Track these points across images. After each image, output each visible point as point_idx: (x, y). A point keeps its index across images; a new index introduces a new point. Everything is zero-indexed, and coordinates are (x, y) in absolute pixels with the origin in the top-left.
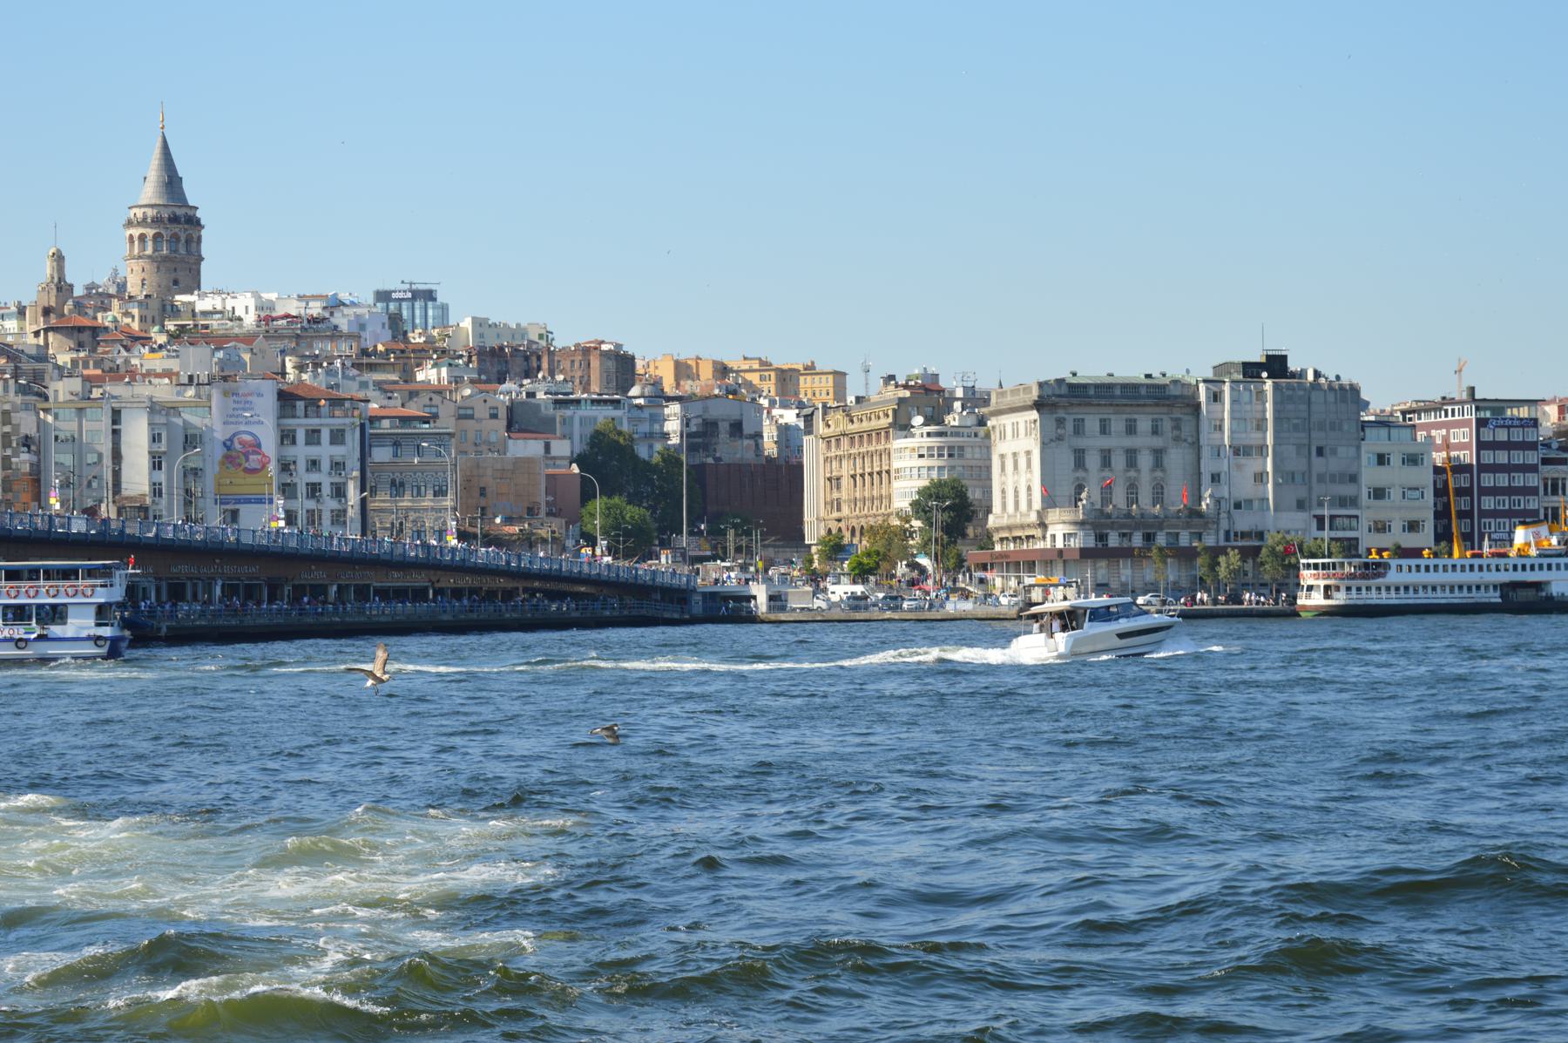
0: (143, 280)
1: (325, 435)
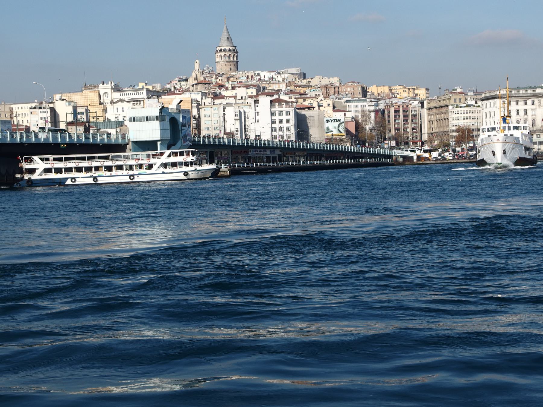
1: (284, 113)
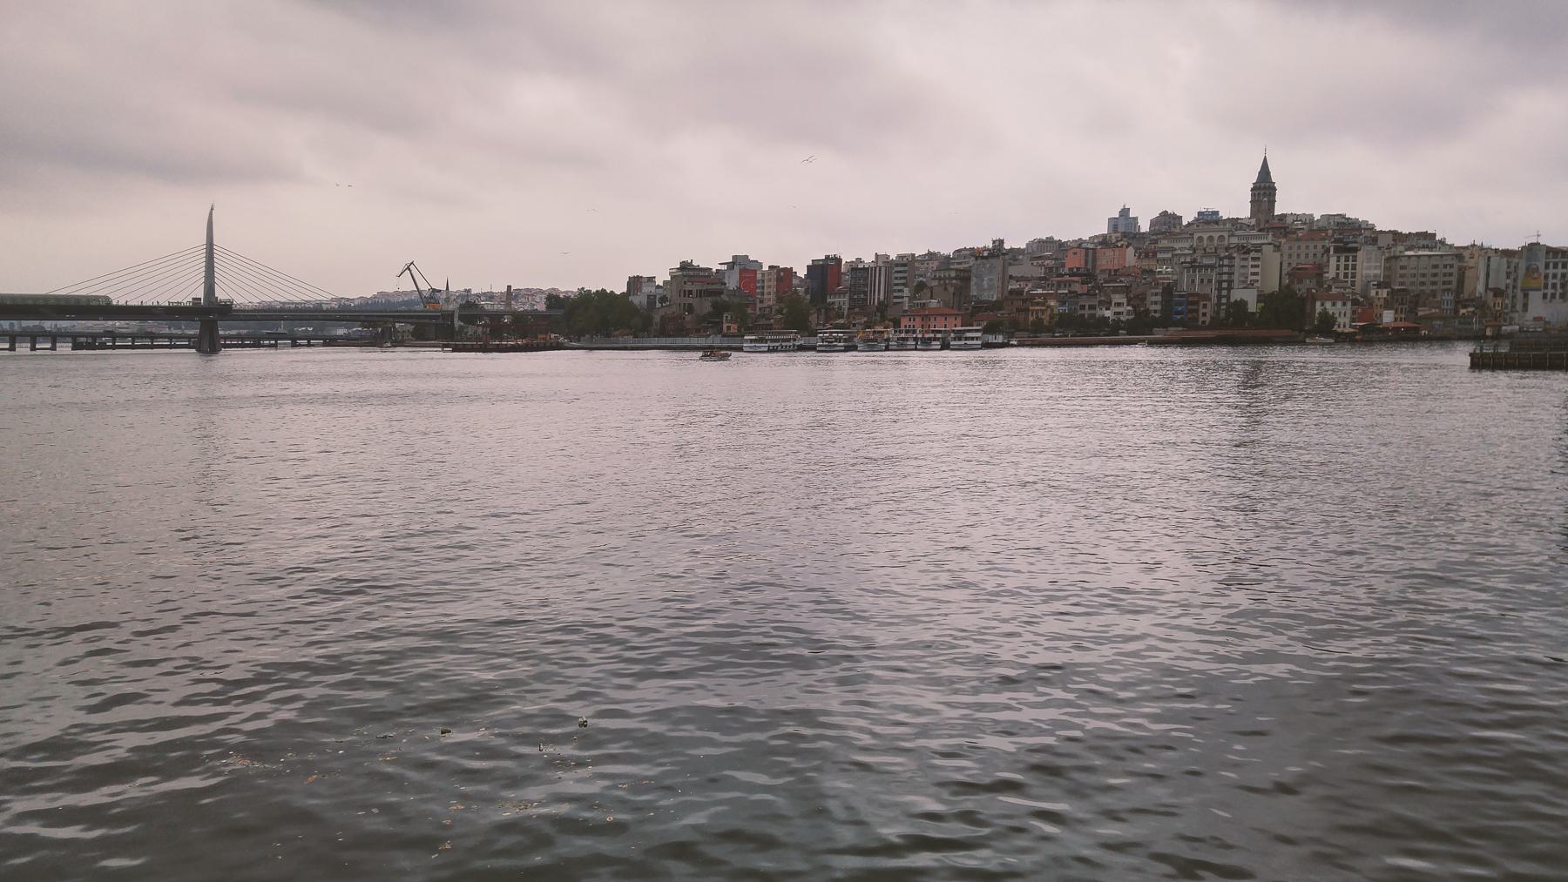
1: (1560, 265)
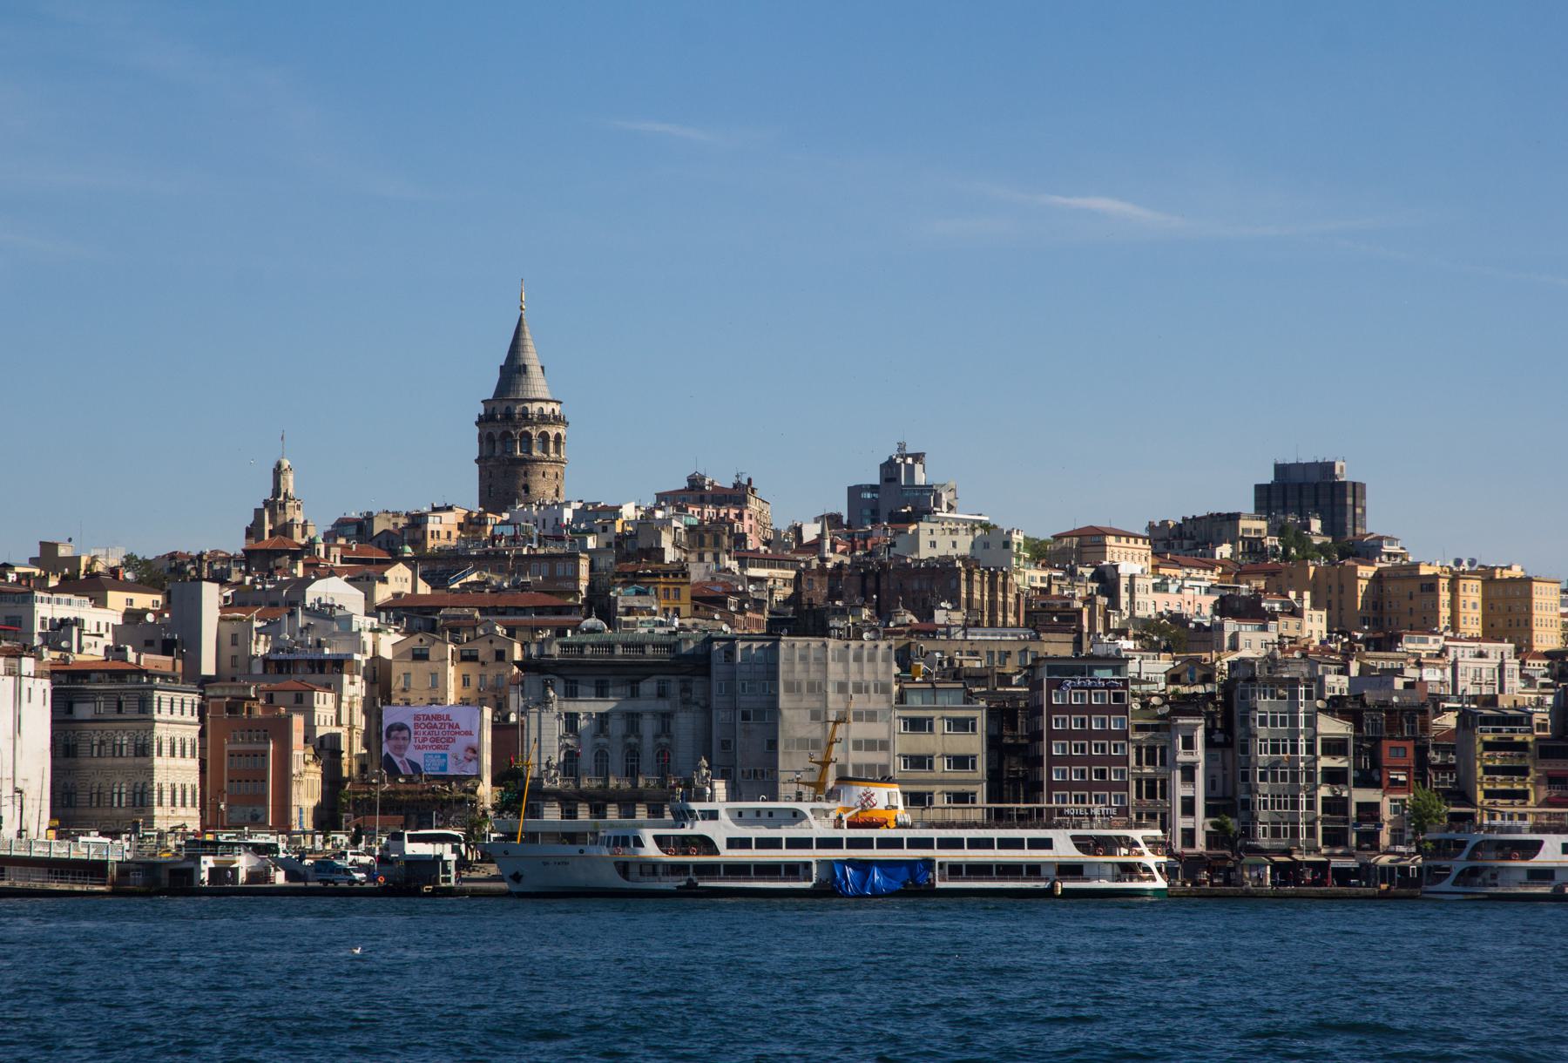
0: (490, 486)
